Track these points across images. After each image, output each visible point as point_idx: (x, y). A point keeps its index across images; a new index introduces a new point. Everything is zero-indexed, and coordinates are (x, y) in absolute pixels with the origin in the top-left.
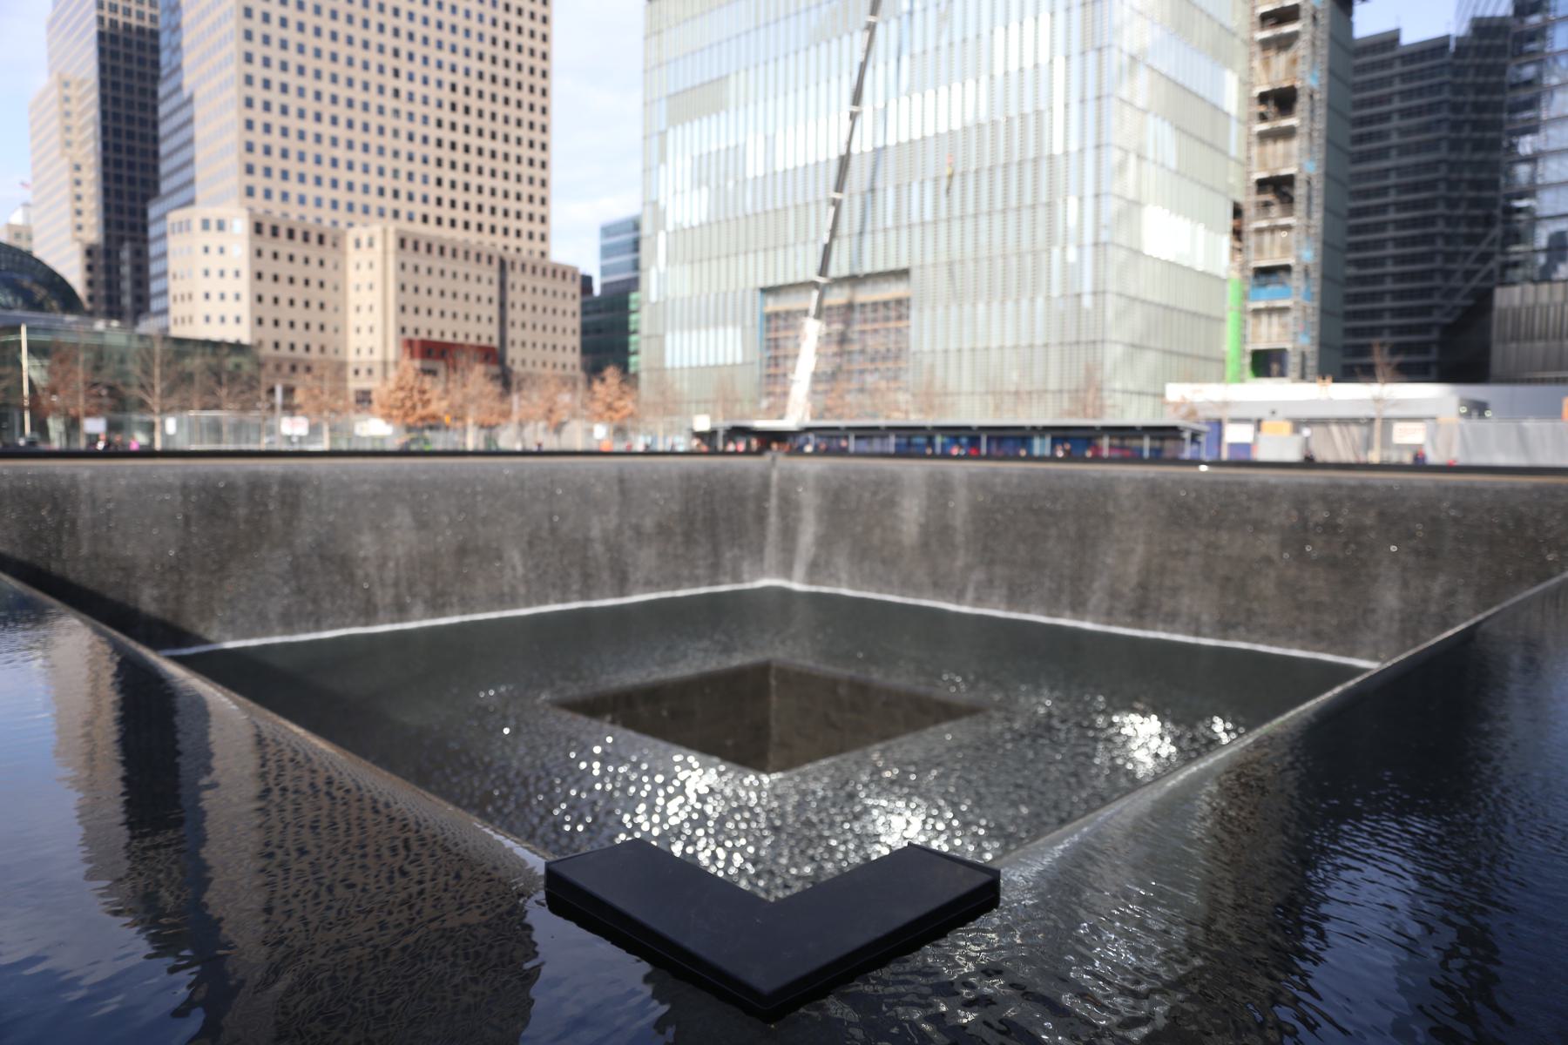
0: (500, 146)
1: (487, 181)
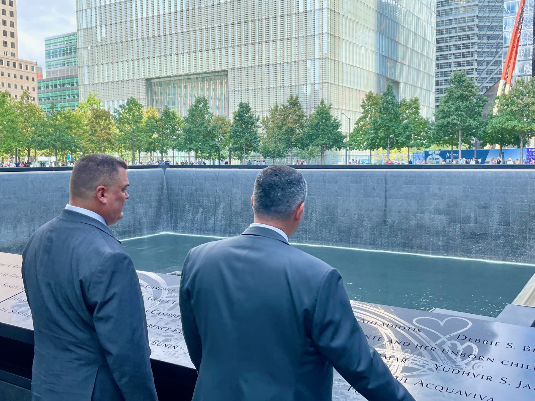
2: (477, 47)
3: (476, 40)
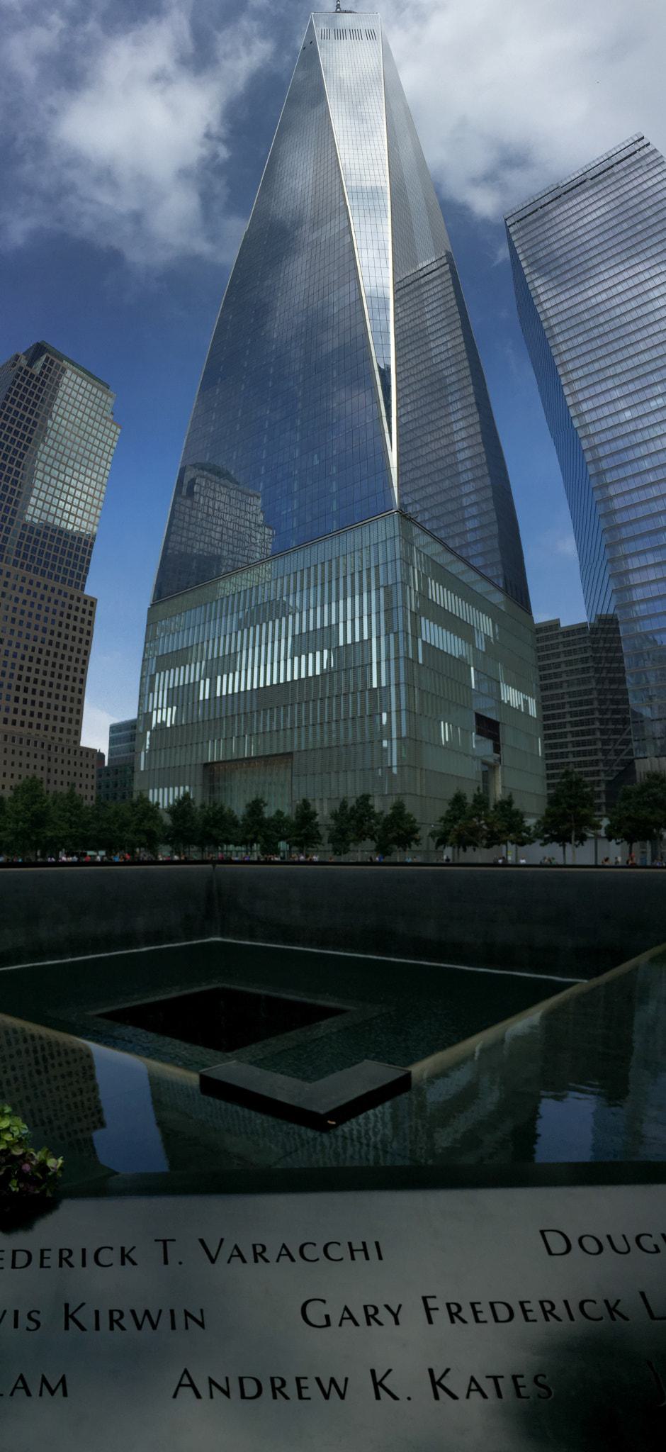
0: (55, 681)
1: (45, 700)
3: (597, 715)
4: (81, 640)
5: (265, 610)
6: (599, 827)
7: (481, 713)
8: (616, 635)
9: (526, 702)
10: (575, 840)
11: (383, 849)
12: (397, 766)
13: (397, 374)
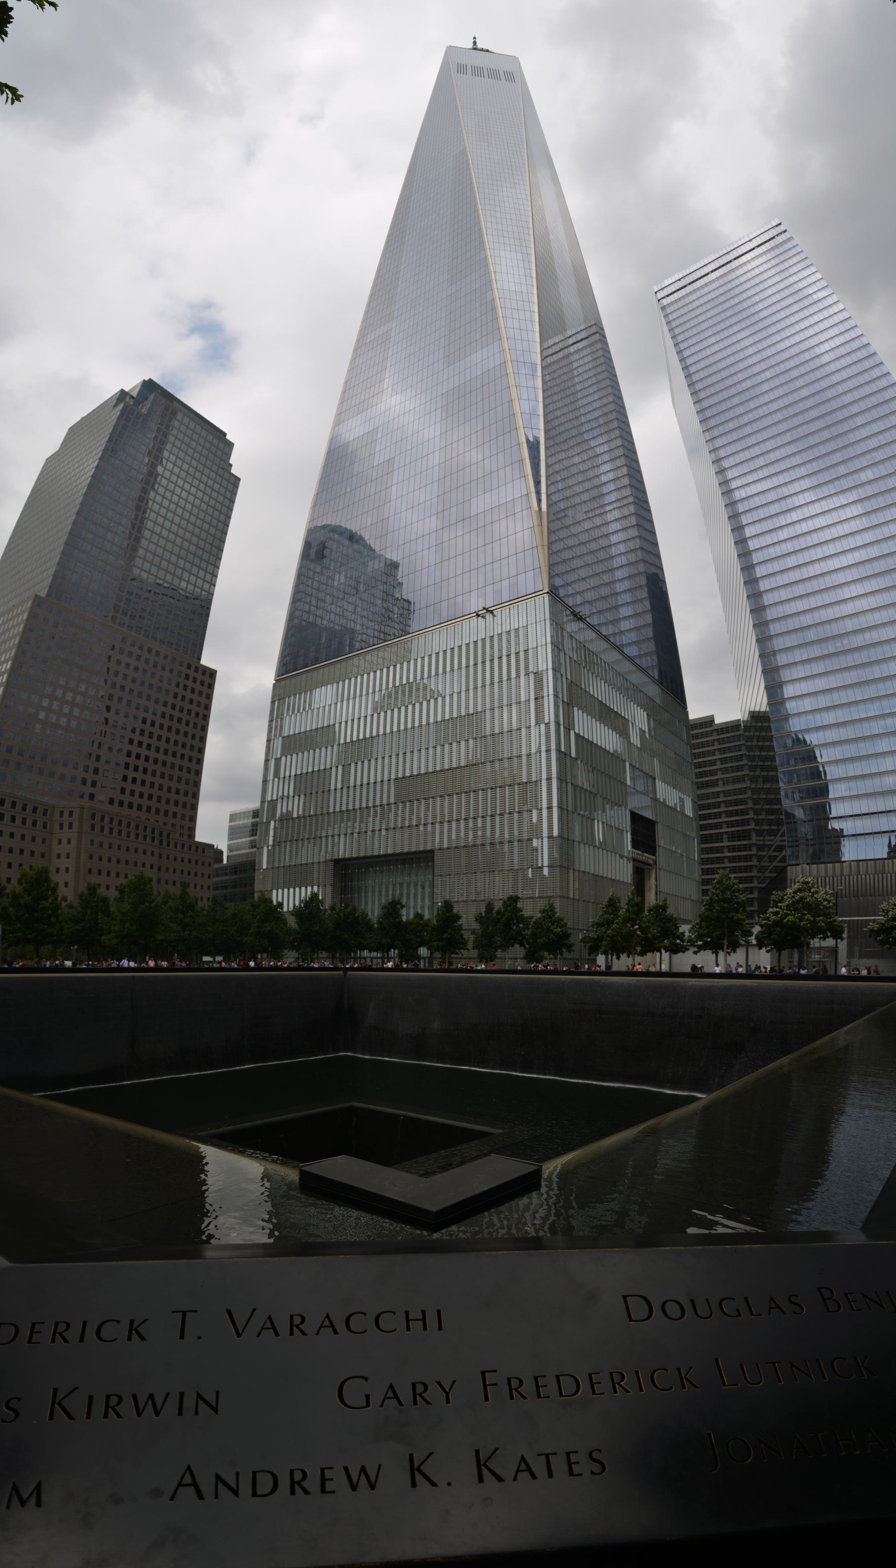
0: (169, 759)
2: (753, 824)
4: (197, 714)
5: (404, 692)
6: (751, 934)
7: (636, 811)
8: (769, 734)
9: (682, 801)
10: (728, 948)
11: (531, 957)
12: (549, 866)
13: (546, 448)
